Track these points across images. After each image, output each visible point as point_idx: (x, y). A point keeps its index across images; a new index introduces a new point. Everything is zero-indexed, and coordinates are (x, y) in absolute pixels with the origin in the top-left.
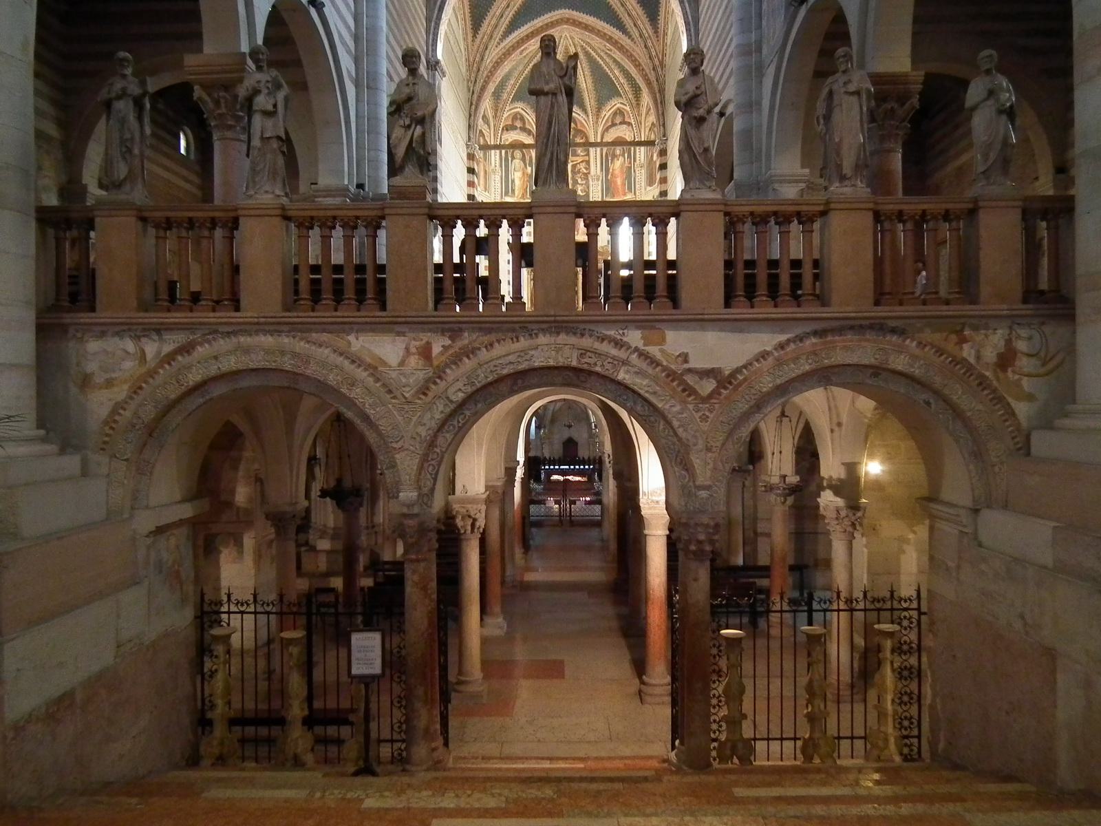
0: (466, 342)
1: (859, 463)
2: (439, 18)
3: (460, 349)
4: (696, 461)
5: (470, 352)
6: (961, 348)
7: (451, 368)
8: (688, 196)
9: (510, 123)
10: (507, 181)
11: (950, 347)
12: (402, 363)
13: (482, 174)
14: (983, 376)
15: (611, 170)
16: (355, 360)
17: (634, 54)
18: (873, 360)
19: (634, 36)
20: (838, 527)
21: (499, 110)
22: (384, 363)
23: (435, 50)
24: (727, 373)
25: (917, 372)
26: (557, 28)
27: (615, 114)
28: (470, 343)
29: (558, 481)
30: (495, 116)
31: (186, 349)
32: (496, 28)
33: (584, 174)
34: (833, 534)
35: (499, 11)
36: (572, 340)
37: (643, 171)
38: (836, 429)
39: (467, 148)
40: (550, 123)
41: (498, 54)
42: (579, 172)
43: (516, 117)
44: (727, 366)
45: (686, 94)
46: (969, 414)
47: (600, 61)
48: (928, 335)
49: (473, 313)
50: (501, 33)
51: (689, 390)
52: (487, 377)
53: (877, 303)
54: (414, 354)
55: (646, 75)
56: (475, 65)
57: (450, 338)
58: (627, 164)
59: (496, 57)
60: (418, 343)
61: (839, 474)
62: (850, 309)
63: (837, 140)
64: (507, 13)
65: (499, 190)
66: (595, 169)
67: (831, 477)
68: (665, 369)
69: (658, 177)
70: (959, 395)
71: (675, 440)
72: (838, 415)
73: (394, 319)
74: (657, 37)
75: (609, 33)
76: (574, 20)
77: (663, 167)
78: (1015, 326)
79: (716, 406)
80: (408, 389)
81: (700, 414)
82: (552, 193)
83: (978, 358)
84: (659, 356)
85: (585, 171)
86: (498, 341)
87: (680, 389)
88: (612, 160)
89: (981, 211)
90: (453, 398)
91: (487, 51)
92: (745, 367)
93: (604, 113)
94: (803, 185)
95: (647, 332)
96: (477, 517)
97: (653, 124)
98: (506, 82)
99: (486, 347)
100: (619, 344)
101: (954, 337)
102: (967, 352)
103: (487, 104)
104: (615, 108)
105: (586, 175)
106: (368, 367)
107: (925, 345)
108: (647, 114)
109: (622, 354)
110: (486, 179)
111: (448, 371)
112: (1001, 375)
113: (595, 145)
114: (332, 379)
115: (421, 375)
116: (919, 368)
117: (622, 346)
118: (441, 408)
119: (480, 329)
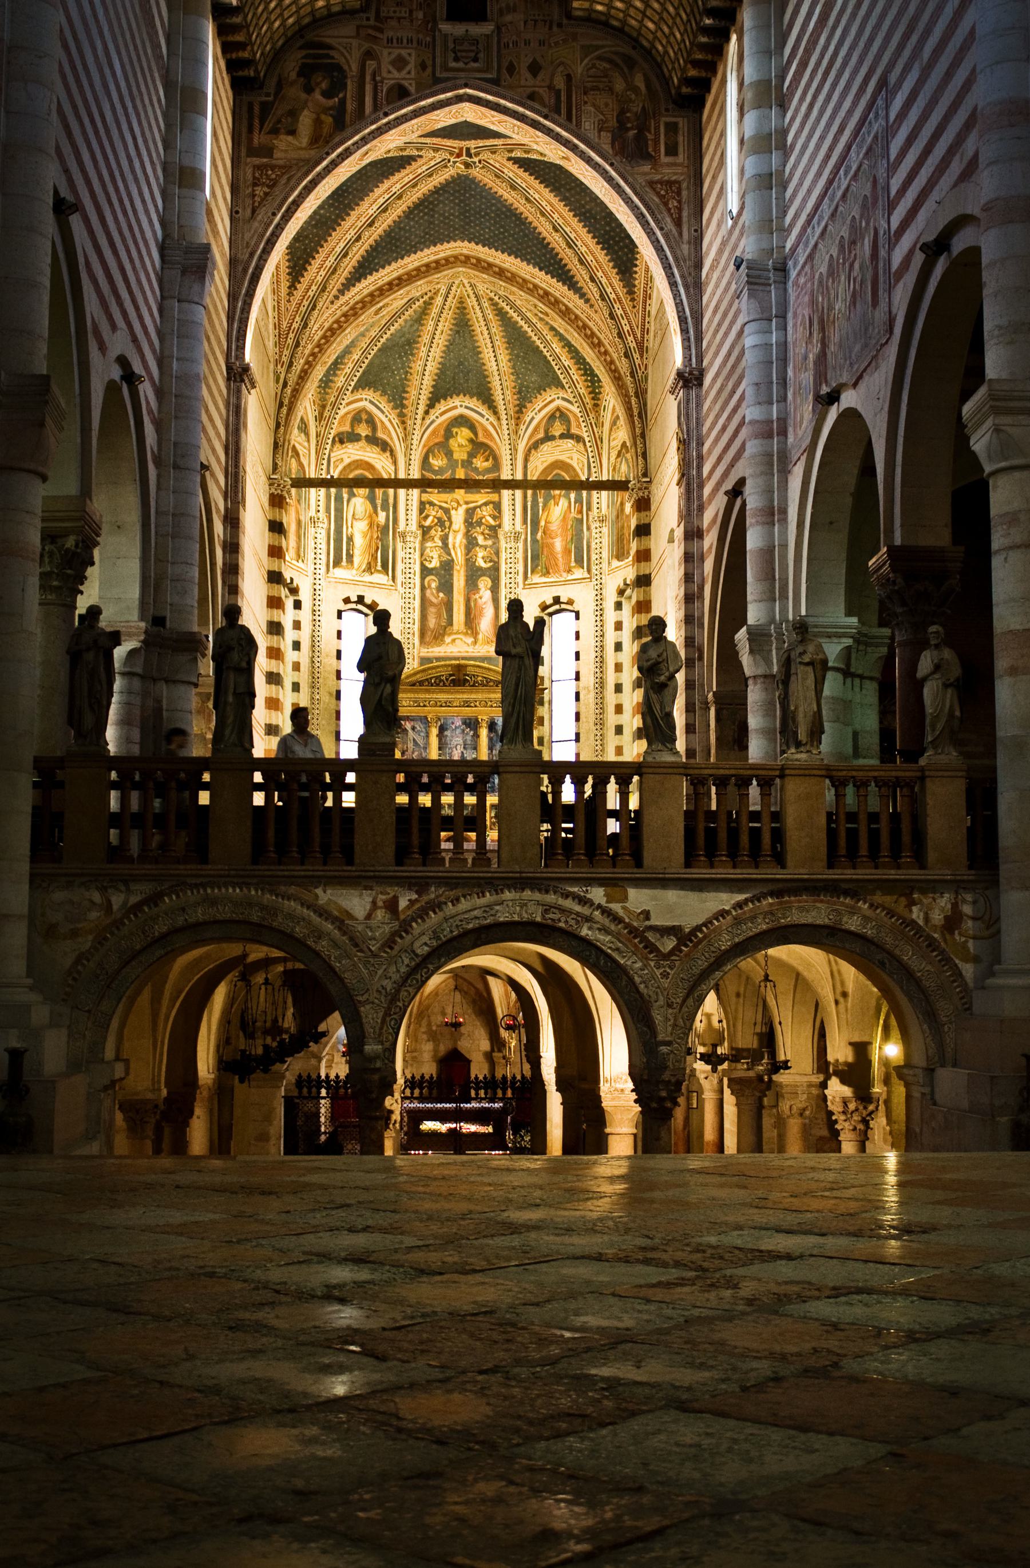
0: (433, 896)
1: (870, 1043)
2: (250, 294)
3: (427, 903)
4: (658, 1017)
5: (436, 906)
6: (911, 911)
7: (417, 922)
8: (650, 759)
9: (347, 428)
10: (338, 541)
11: (901, 909)
12: (369, 917)
14: (935, 939)
15: (542, 523)
16: (323, 913)
17: (591, 324)
18: (827, 921)
19: (590, 296)
20: (846, 1124)
22: (351, 917)
23: (241, 348)
24: (687, 930)
25: (869, 932)
26: (446, 273)
27: (552, 417)
28: (437, 897)
29: (434, 1134)
30: (319, 418)
31: (154, 899)
32: (333, 273)
34: (842, 1134)
35: (342, 245)
36: (537, 896)
37: (605, 530)
38: (841, 1000)
40: (517, 685)
41: (334, 313)
42: (479, 523)
43: (357, 418)
44: (688, 923)
45: (648, 661)
46: (919, 974)
48: (878, 898)
49: (441, 869)
50: (342, 280)
51: (651, 947)
52: (452, 932)
53: (830, 865)
54: (381, 908)
55: (612, 362)
56: (291, 335)
57: (417, 892)
58: (574, 514)
59: (331, 320)
60: (384, 897)
61: (846, 1056)
62: (802, 871)
63: (792, 708)
64: (355, 249)
66: (512, 519)
67: (837, 1061)
68: (627, 926)
69: (634, 546)
70: (908, 955)
71: (637, 996)
72: (843, 983)
73: (363, 874)
74: (633, 300)
75: (544, 285)
76: (479, 260)
77: (643, 530)
78: (961, 891)
79: (677, 963)
80: (374, 942)
81: (661, 971)
82: (517, 752)
83: (927, 919)
84: (621, 913)
85: (492, 522)
86: (464, 896)
87: (641, 946)
88: (545, 505)
89: (928, 780)
90: (419, 951)
91: (316, 313)
92: (705, 924)
93: (531, 415)
94: (849, 642)
95: (609, 889)
96: (392, 1108)
97: (624, 445)
99: (452, 902)
100: (583, 901)
101: (903, 901)
102: (916, 914)
103: (306, 407)
104: (552, 406)
105: (494, 531)
106: (336, 918)
107: (877, 908)
108: (614, 423)
109: (586, 911)
110: (299, 537)
111: (414, 924)
112: (948, 937)
113: (511, 484)
114: (299, 931)
115: (387, 929)
116: (871, 929)
117: (585, 903)
118: (406, 961)
119: (447, 884)
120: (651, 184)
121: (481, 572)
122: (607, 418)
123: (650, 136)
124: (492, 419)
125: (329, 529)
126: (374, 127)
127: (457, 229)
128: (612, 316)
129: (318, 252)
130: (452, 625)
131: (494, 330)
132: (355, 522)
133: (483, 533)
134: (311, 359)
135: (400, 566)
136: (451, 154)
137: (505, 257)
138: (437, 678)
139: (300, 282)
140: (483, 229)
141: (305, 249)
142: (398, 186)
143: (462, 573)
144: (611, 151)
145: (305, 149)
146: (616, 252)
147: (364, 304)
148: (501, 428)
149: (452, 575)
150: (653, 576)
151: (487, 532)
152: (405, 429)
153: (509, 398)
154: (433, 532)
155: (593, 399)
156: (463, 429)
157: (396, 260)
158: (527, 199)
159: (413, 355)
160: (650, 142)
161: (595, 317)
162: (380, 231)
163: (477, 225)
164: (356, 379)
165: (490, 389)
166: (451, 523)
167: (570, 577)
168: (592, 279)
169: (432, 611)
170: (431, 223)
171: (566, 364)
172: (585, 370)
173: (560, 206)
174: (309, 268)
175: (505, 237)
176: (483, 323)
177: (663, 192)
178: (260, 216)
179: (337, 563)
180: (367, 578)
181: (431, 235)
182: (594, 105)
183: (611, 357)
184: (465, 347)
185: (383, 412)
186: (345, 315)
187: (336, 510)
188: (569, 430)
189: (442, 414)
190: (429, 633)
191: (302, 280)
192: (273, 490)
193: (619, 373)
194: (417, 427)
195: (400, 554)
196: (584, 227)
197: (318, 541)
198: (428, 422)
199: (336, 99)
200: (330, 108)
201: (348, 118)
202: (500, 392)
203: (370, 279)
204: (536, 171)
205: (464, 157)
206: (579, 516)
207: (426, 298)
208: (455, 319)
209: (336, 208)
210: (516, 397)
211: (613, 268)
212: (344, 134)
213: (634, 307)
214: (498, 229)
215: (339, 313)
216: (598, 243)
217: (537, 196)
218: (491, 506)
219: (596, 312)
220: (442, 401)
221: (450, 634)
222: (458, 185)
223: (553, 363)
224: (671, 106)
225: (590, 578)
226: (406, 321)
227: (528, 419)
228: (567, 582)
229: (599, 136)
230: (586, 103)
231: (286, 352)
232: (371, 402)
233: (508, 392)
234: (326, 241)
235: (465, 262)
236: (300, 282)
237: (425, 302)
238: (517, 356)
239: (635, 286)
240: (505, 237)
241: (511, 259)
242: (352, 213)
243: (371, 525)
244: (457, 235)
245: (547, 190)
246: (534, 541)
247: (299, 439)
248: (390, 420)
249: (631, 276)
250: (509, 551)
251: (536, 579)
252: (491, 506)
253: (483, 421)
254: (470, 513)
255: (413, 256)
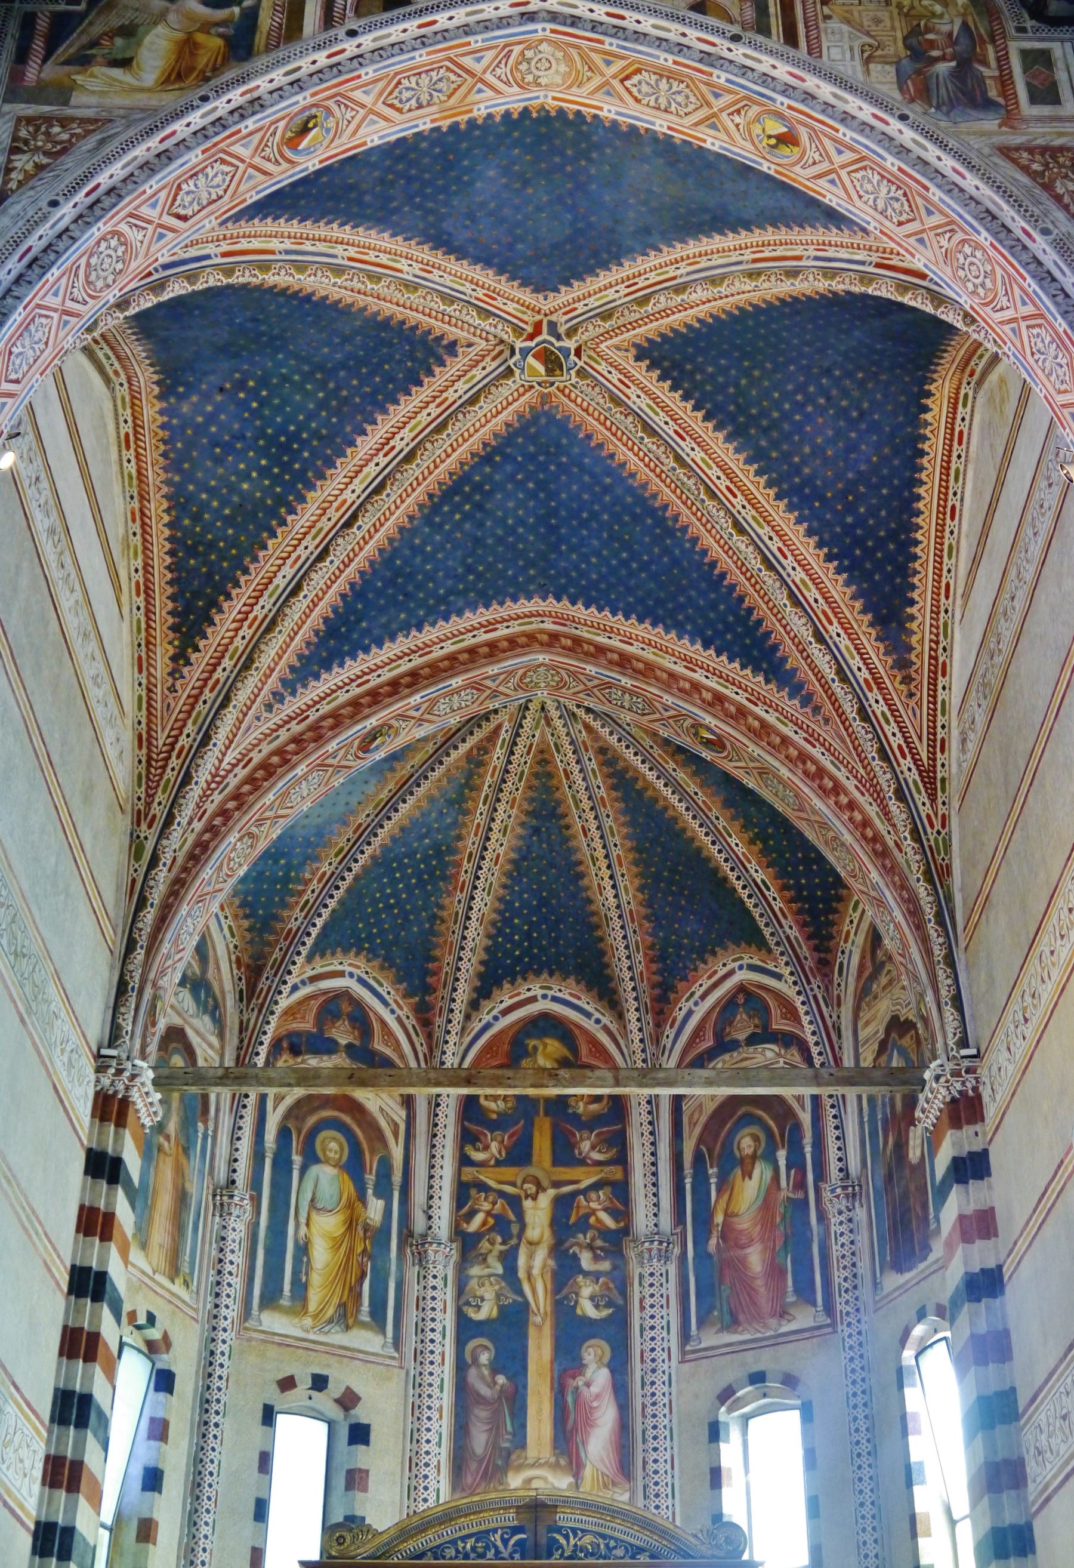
9: (306, 1025)
10: (275, 1252)
13: (165, 1202)
15: (719, 1219)
17: (816, 752)
21: (268, 972)
27: (728, 1007)
32: (269, 629)
33: (604, 1233)
35: (288, 571)
37: (860, 1214)
39: (100, 1069)
42: (583, 1224)
47: (674, 799)
50: (290, 658)
55: (866, 823)
56: (174, 762)
59: (267, 748)
65: (237, 1282)
74: (907, 680)
75: (713, 683)
76: (577, 641)
91: (230, 716)
93: (685, 1006)
98: (303, 864)
108: (864, 994)
120: (1006, 152)
121: (589, 1328)
122: (848, 986)
123: (990, 72)
124: (605, 1020)
125: (257, 1224)
126: (322, 58)
127: (532, 564)
128: (864, 714)
129: (237, 585)
130: (523, 1446)
131: (608, 823)
132: (314, 1216)
133: (591, 1247)
134: (218, 821)
135: (411, 1315)
136: (518, 331)
137: (633, 627)
138: (481, 1536)
139: (197, 649)
140: (585, 558)
141: (210, 575)
142: (407, 433)
143: (547, 1330)
144: (897, 95)
145: (149, 90)
146: (868, 576)
147: (338, 720)
148: (625, 1035)
149: (525, 1336)
150: (1007, 1272)
151: (599, 1243)
152: (429, 1036)
153: (641, 968)
154: (484, 1245)
155: (816, 949)
156: (548, 1041)
157: (406, 628)
158: (678, 459)
159: (444, 878)
160: (988, 82)
161: (825, 733)
162: (370, 548)
163: (572, 549)
164: (326, 913)
165: (603, 953)
166: (523, 1227)
167: (785, 1329)
168: (820, 638)
169: (481, 1413)
170: (478, 541)
171: (759, 877)
172: (799, 888)
173: (748, 476)
174: (217, 619)
175: (631, 574)
176: (586, 804)
177: (1036, 167)
178: (18, 208)
179: (270, 1299)
180: (338, 1337)
181: (479, 576)
182: (848, 22)
183: (861, 812)
184: (552, 865)
185: (385, 1003)
186: (297, 740)
187: (274, 1184)
188: (766, 1026)
189: (506, 1012)
190: (473, 1466)
191: (202, 644)
192: (106, 1081)
193: (884, 844)
194: (455, 1027)
195: (413, 1290)
196: (799, 521)
197: (230, 1245)
198: (477, 1026)
199: (236, 10)
200: (218, 24)
201: (260, 39)
202: (622, 952)
203: (352, 668)
204: (696, 386)
205: (545, 336)
206: (800, 1195)
207: (471, 741)
208: (531, 800)
209: (277, 480)
210: (654, 967)
211: (864, 611)
212: (247, 67)
213: (911, 695)
214: (616, 554)
215: (284, 735)
216: (829, 558)
217: (699, 455)
218: (608, 1190)
219: (827, 721)
220: (507, 986)
221: (519, 1468)
222: (533, 439)
223: (732, 876)
224: (1029, 24)
225: (833, 1325)
226: (431, 799)
227: (680, 1015)
228: (778, 1340)
229: (868, 72)
230: (827, 17)
231: (160, 796)
232: (361, 981)
233: (640, 957)
234: (255, 559)
235: (550, 645)
236: (197, 649)
237: (469, 755)
238: (657, 878)
239: (911, 649)
240: (631, 574)
241: (643, 630)
242: (310, 495)
243: (351, 1224)
244: (531, 580)
245: (721, 436)
246: (702, 1255)
247: (196, 1022)
248: (399, 1020)
249: (902, 627)
250: (648, 1280)
251: (711, 1338)
252: (608, 1190)
253: (588, 1024)
254: (563, 1205)
255: (442, 628)
